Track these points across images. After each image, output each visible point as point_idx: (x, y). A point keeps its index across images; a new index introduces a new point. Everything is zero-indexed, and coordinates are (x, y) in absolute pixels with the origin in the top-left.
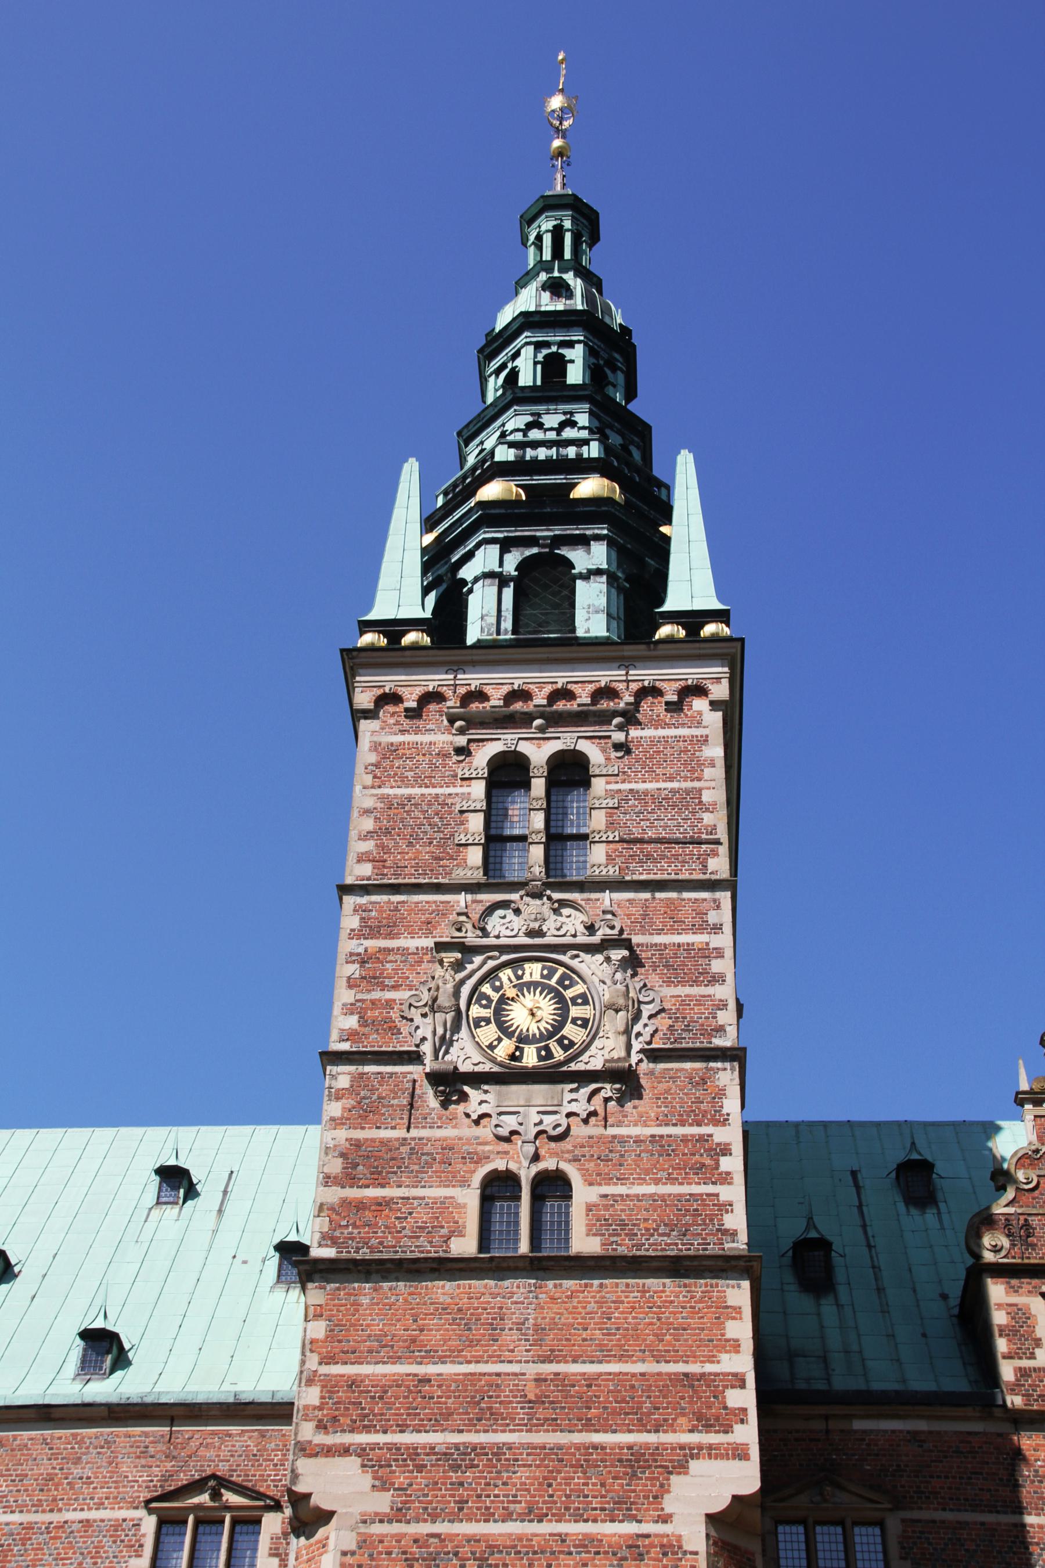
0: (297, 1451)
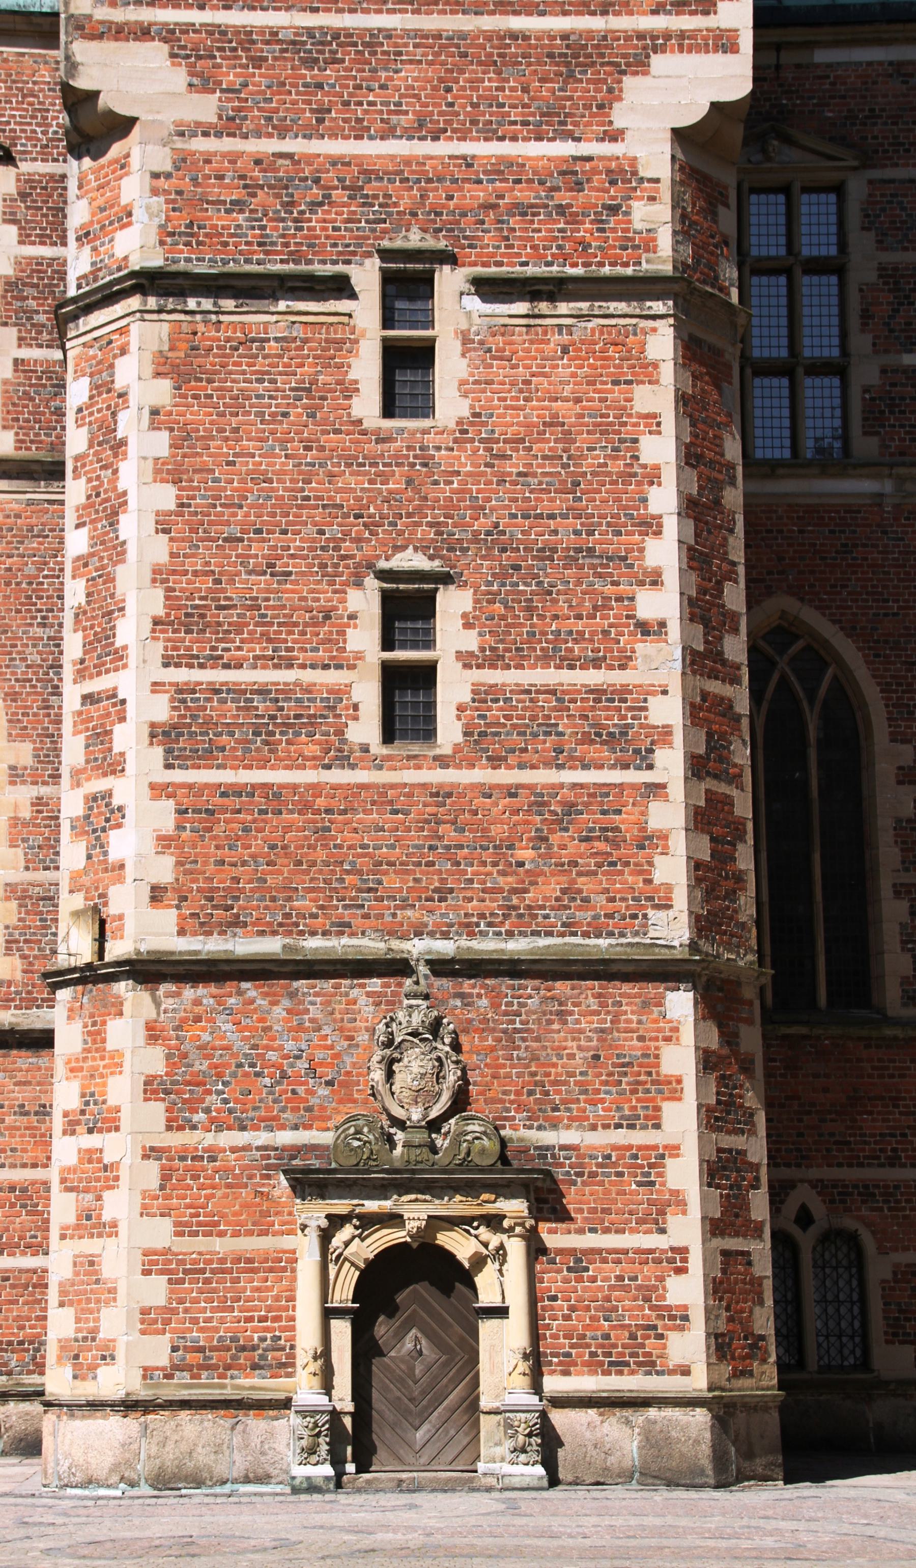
0: (70, 29)
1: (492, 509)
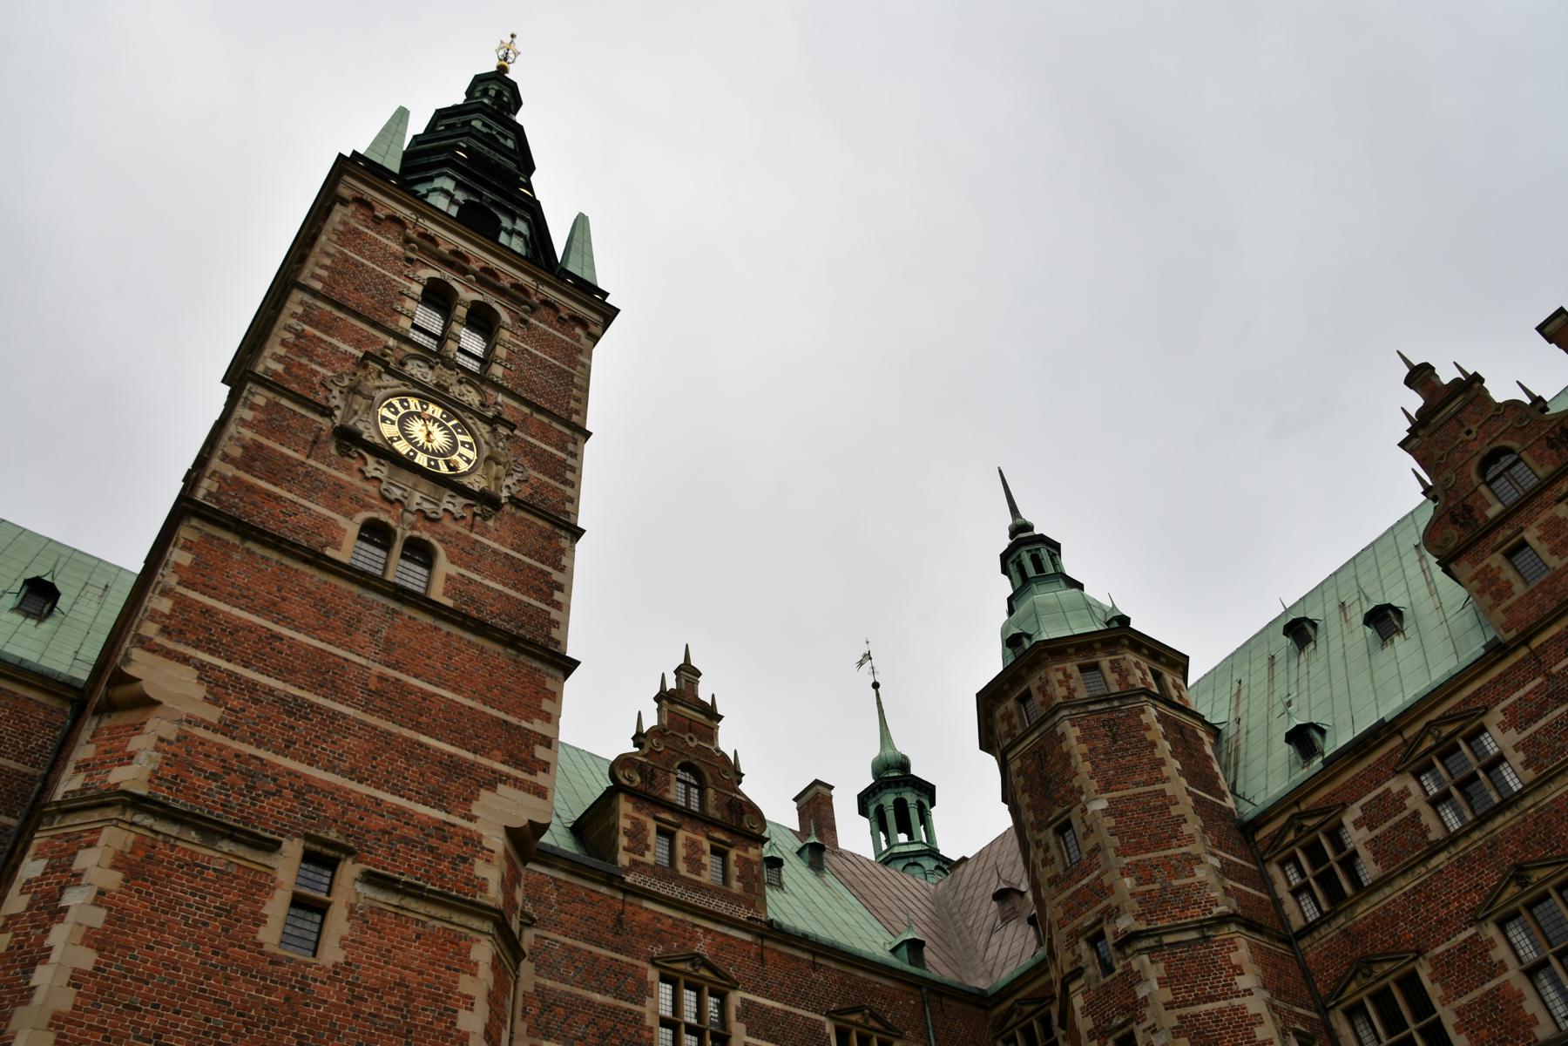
0: (135, 641)
1: (345, 1035)
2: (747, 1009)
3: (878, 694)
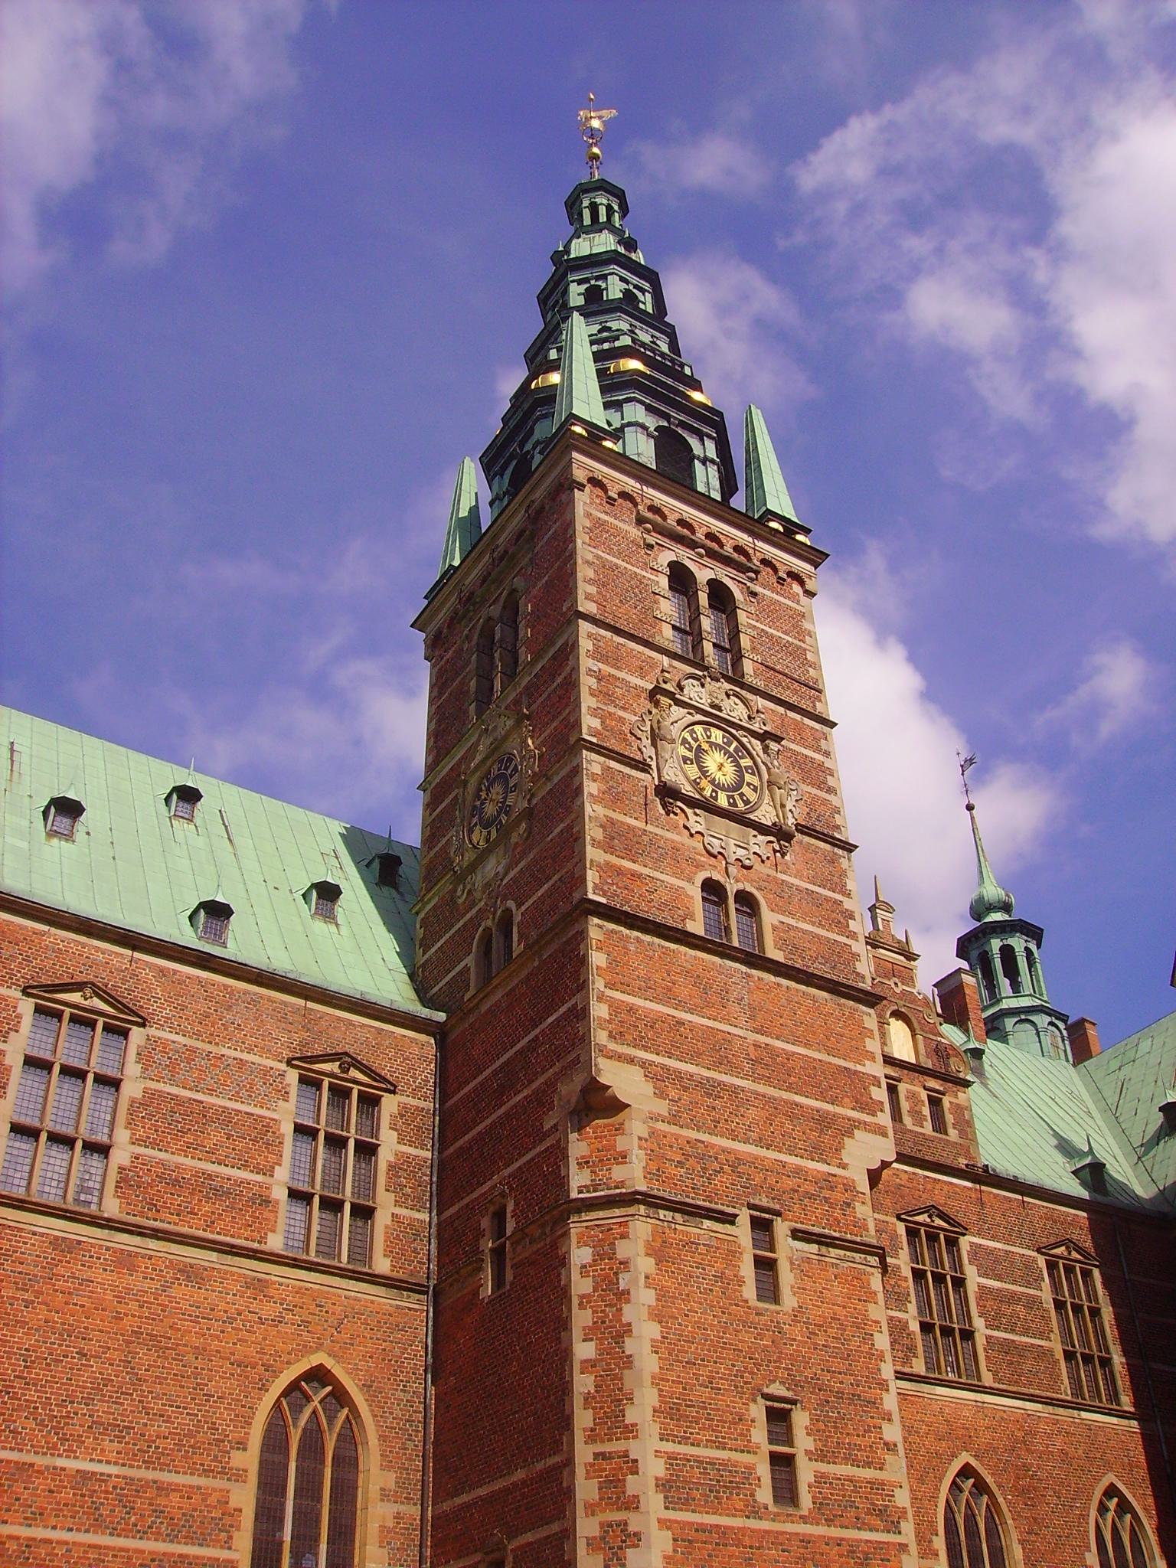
2: (976, 1251)
3: (972, 818)
